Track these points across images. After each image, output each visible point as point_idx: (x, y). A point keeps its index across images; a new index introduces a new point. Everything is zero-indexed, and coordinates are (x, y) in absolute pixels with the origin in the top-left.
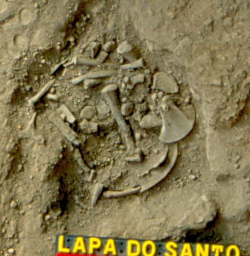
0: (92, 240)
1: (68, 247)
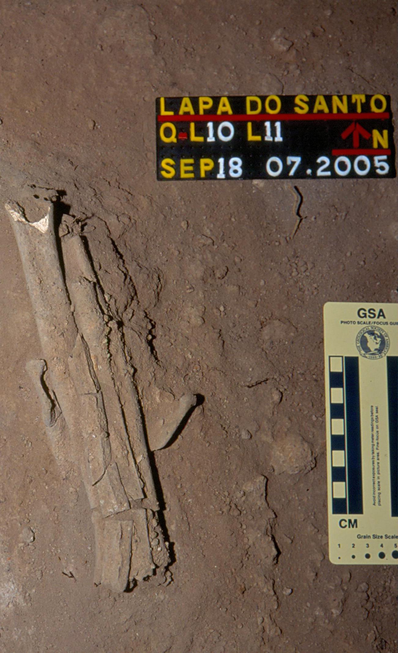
0: (201, 100)
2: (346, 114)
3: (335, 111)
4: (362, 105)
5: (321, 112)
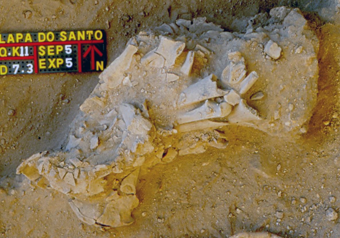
1: (5, 41)
3: (79, 39)
4: (91, 35)
5: (72, 40)
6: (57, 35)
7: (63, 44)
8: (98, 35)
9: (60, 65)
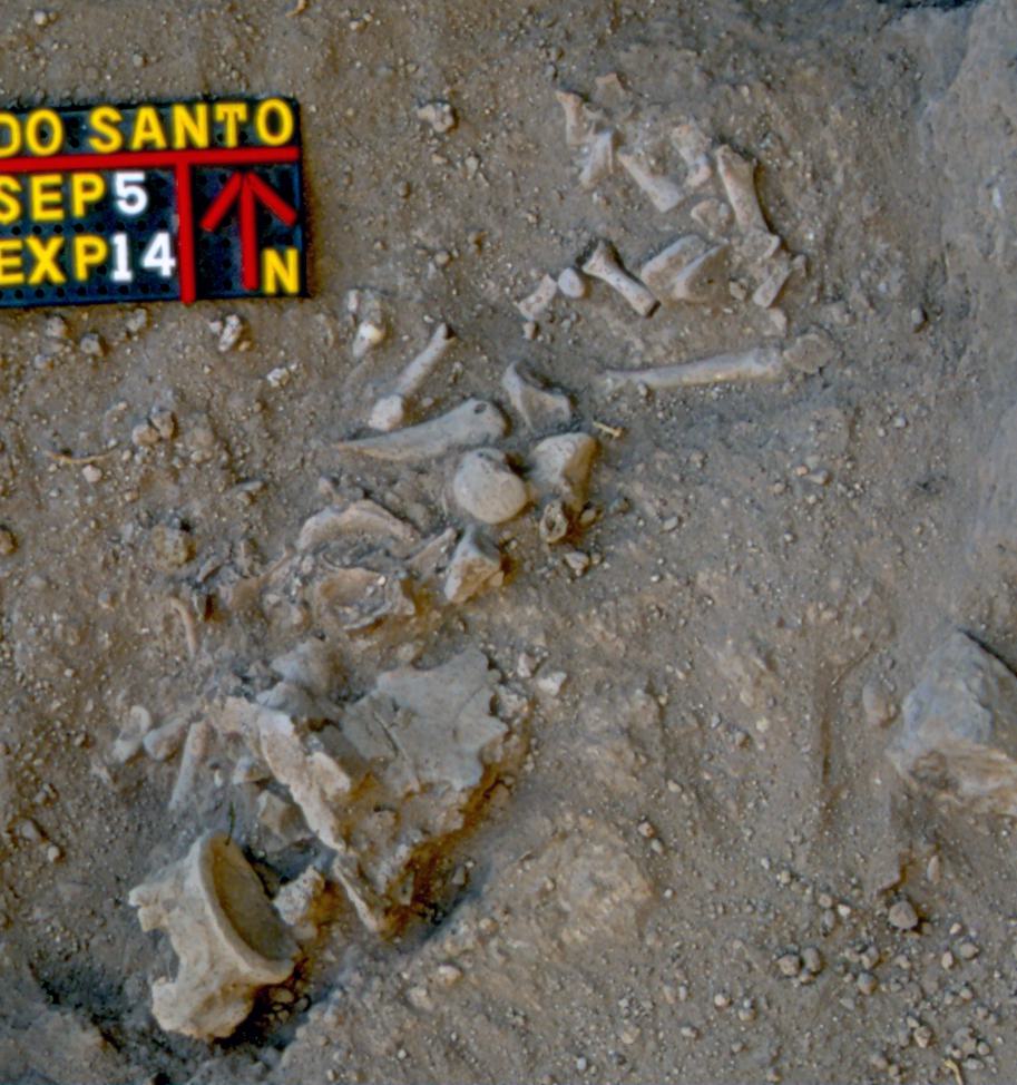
2: (203, 150)
3: (180, 143)
5: (148, 147)
6: (75, 129)
7: (107, 166)
8: (274, 123)
9: (91, 269)
